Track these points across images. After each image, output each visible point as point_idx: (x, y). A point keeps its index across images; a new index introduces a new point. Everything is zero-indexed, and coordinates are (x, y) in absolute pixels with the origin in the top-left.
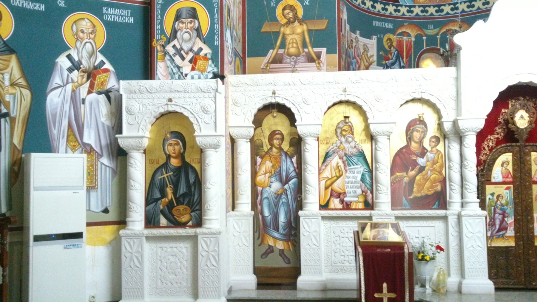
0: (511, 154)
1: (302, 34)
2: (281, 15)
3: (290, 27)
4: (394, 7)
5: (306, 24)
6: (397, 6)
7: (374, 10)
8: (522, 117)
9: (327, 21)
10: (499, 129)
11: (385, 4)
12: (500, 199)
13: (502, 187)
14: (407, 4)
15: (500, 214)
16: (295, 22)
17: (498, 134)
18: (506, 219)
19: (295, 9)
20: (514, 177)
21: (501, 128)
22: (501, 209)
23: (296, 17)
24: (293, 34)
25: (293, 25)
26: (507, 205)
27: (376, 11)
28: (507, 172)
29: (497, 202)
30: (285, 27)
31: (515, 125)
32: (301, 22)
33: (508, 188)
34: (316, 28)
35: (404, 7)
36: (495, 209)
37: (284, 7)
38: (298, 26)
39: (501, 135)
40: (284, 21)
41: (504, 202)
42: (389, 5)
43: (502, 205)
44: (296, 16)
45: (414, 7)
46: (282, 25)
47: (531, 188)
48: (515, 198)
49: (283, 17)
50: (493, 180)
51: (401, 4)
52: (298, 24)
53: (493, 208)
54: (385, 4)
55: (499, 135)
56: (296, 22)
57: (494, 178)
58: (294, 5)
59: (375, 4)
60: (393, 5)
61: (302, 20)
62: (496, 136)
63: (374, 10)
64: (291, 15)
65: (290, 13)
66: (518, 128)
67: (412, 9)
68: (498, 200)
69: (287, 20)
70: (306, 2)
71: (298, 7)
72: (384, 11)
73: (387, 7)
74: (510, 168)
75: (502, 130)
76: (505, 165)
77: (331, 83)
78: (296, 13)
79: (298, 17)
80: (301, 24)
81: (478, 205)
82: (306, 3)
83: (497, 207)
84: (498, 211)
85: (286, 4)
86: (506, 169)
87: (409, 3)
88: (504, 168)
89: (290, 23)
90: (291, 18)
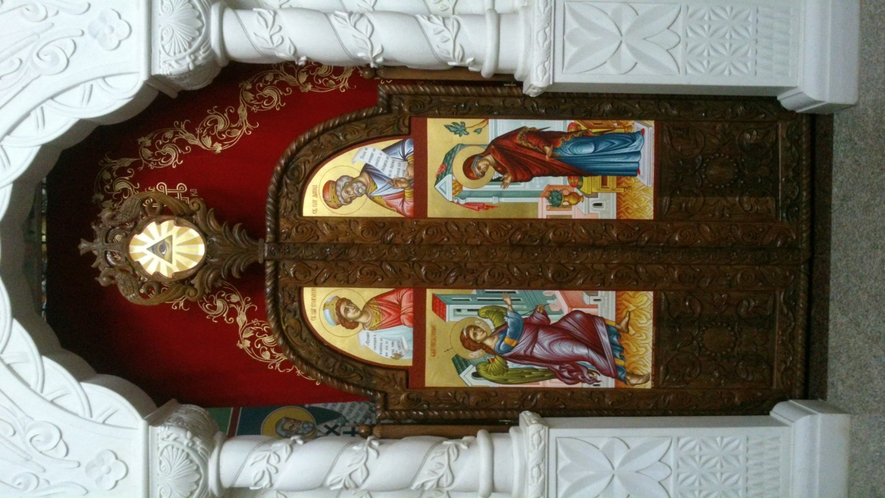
0: (307, 292)
8: (160, 249)
10: (214, 308)
12: (479, 337)
13: (434, 329)
15: (535, 340)
17: (233, 313)
18: (554, 319)
20: (397, 284)
21: (211, 300)
22: (516, 336)
26: (500, 313)
28: (374, 311)
29: (488, 350)
31: (193, 276)
33: (439, 307)
36: (516, 358)
39: (238, 304)
41: (491, 324)
43: (501, 330)
47: (445, 223)
48: (477, 285)
50: (407, 360)
53: (511, 365)
55: (238, 309)
57: (398, 356)
62: (242, 319)
66: (204, 264)
68: (481, 346)
74: (361, 296)
75: (219, 297)
76: (351, 315)
81: (499, 442)
83: (509, 348)
84: (521, 347)
86: (363, 312)
88: (363, 319)
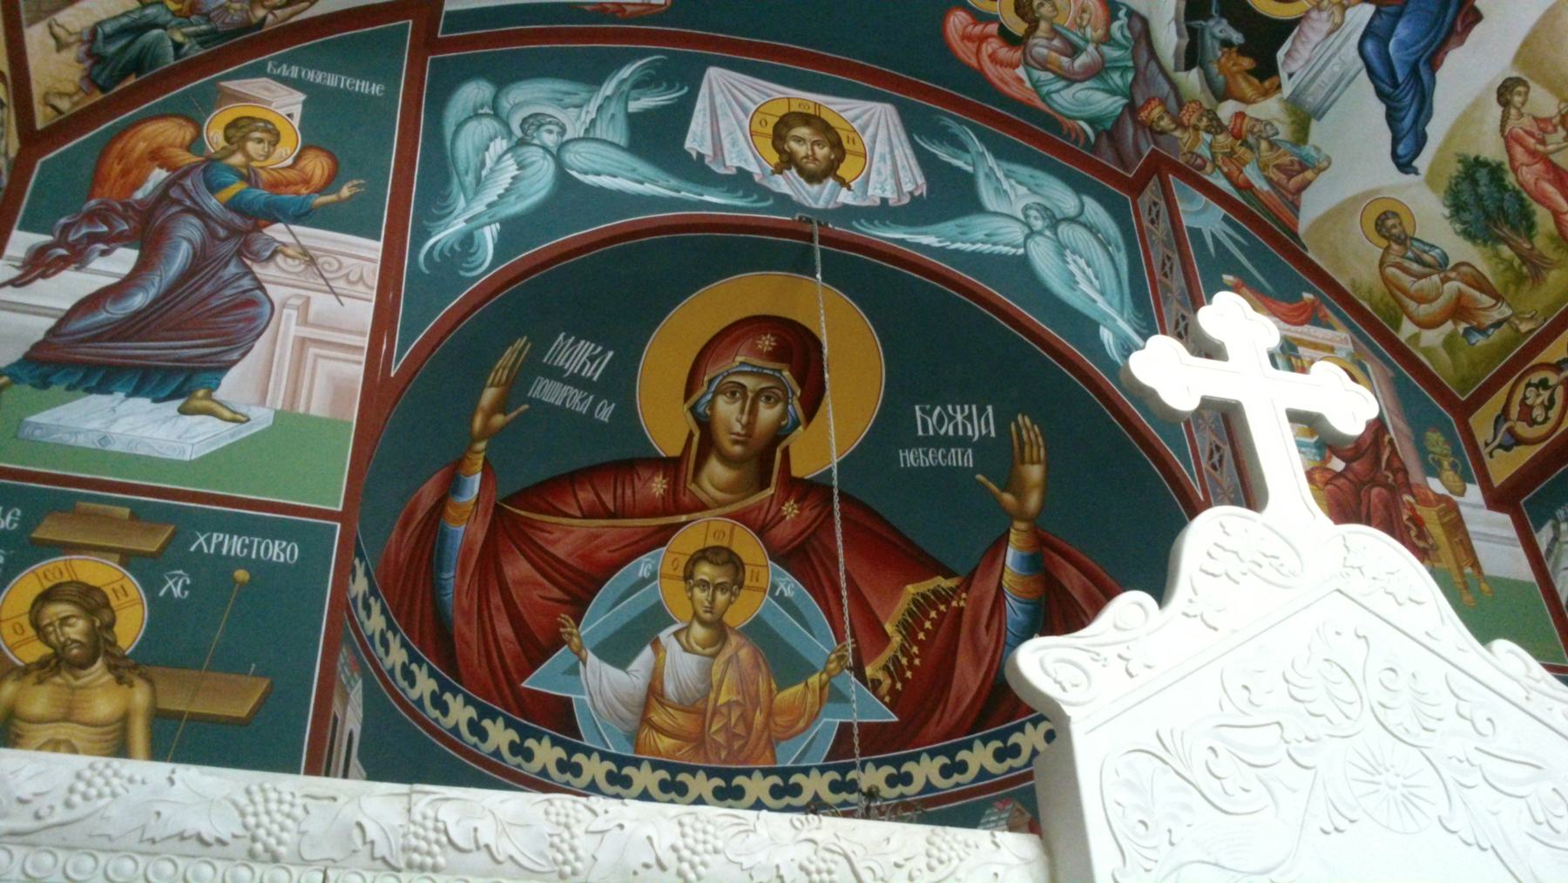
1: (118, 725)
2: (25, 620)
3: (59, 685)
4: (560, 753)
5: (150, 681)
6: (572, 749)
7: (480, 745)
9: (263, 684)
11: (525, 733)
14: (608, 747)
16: (92, 661)
19: (107, 604)
23: (100, 644)
24: (67, 718)
25: (77, 678)
27: (486, 748)
30: (32, 678)
32: (123, 669)
34: (203, 707)
35: (596, 756)
37: (48, 585)
38: (102, 686)
40: (35, 651)
42: (539, 737)
44: (106, 641)
45: (637, 763)
46: (15, 668)
49: (30, 632)
51: (586, 743)
52: (108, 677)
54: (525, 733)
56: (99, 663)
58: (108, 591)
59: (487, 723)
60: (555, 742)
61: (132, 661)
63: (480, 745)
64: (77, 630)
65: (73, 621)
67: (627, 770)
69: (50, 651)
70: (171, 583)
71: (123, 599)
72: (519, 760)
73: (531, 743)
77: (216, 848)
78: (110, 626)
79: (114, 644)
80: (120, 680)
82: (170, 591)
85: (66, 578)
87: (616, 749)
89: (63, 663)
90: (75, 641)
